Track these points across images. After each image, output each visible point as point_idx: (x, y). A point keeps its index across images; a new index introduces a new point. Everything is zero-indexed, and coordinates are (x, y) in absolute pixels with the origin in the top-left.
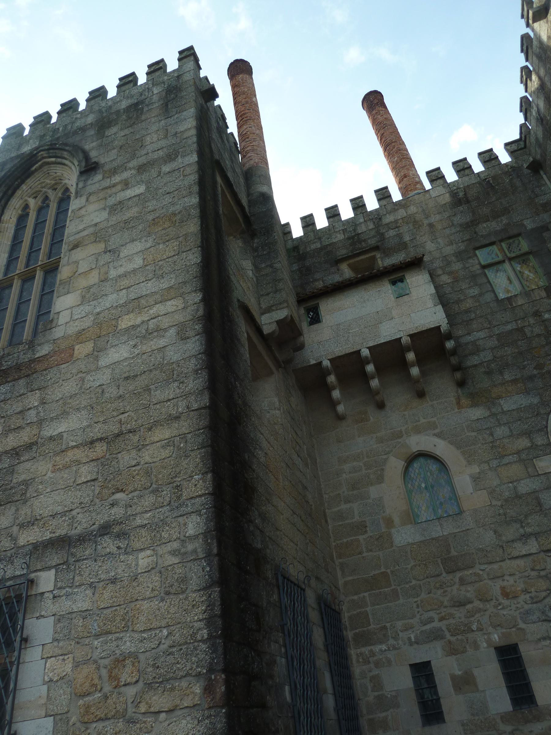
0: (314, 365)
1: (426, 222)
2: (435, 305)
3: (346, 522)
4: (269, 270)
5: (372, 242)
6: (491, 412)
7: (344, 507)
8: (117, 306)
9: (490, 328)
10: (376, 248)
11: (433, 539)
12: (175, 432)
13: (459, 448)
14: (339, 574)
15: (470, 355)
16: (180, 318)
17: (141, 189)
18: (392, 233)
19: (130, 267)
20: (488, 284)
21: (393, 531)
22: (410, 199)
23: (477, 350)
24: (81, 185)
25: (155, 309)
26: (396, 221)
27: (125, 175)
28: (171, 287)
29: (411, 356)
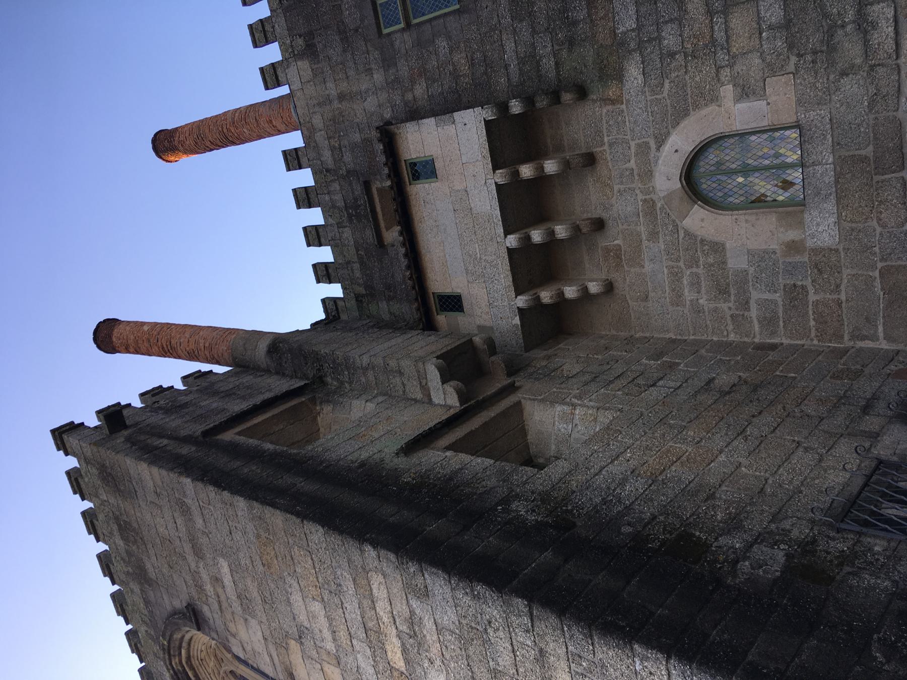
0: (521, 319)
1: (336, 104)
2: (454, 123)
3: (781, 315)
4: (370, 374)
5: (358, 189)
6: (634, 50)
7: (754, 313)
8: (374, 661)
9: (501, 32)
10: (367, 185)
11: (837, 182)
12: (563, 664)
13: (686, 114)
14: (868, 344)
15: (539, 71)
16: (397, 587)
17: (224, 567)
18: (348, 157)
19: (322, 622)
20: (434, 23)
21: (810, 243)
22: (302, 121)
23: (530, 59)
24: (214, 635)
25: (381, 613)
26: (332, 149)
27: (205, 576)
28: (354, 580)
29: (526, 171)
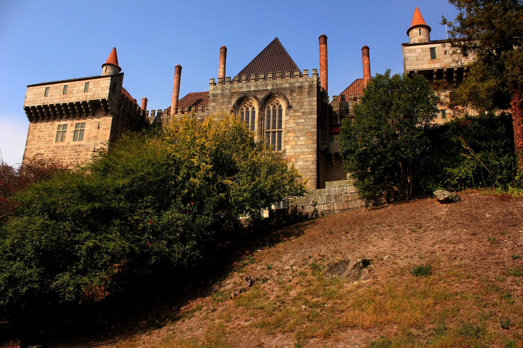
16: (312, 159)
17: (303, 121)
27: (300, 114)
